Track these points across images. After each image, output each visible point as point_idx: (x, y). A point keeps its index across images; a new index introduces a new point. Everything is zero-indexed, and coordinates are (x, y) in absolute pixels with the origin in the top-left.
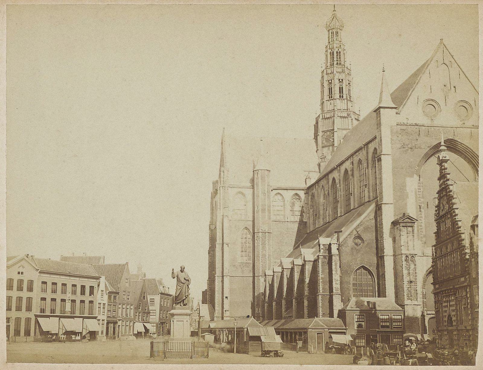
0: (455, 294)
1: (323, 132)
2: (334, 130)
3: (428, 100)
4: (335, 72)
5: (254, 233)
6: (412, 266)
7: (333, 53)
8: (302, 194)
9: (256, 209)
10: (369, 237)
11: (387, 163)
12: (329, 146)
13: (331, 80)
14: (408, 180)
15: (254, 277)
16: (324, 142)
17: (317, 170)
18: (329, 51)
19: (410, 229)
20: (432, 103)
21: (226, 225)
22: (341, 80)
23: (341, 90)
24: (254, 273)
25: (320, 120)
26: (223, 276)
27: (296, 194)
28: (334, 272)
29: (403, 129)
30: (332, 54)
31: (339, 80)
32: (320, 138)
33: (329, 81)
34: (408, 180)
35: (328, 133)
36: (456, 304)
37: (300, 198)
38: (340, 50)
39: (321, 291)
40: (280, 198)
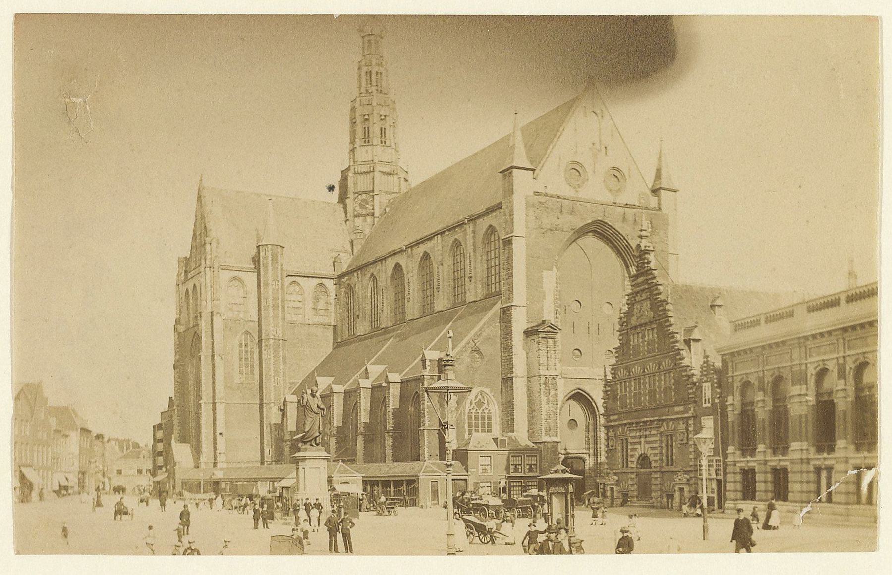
1: (355, 193)
2: (373, 191)
3: (614, 168)
4: (374, 104)
5: (260, 341)
6: (552, 392)
8: (329, 284)
9: (263, 303)
10: (493, 350)
11: (519, 249)
12: (365, 216)
15: (261, 405)
16: (357, 208)
17: (349, 247)
18: (365, 69)
20: (576, 169)
23: (383, 131)
24: (261, 400)
25: (350, 174)
26: (214, 404)
27: (321, 285)
29: (542, 201)
34: (545, 273)
35: (364, 196)
36: (661, 441)
37: (326, 292)
38: (382, 70)
39: (427, 425)
40: (297, 288)
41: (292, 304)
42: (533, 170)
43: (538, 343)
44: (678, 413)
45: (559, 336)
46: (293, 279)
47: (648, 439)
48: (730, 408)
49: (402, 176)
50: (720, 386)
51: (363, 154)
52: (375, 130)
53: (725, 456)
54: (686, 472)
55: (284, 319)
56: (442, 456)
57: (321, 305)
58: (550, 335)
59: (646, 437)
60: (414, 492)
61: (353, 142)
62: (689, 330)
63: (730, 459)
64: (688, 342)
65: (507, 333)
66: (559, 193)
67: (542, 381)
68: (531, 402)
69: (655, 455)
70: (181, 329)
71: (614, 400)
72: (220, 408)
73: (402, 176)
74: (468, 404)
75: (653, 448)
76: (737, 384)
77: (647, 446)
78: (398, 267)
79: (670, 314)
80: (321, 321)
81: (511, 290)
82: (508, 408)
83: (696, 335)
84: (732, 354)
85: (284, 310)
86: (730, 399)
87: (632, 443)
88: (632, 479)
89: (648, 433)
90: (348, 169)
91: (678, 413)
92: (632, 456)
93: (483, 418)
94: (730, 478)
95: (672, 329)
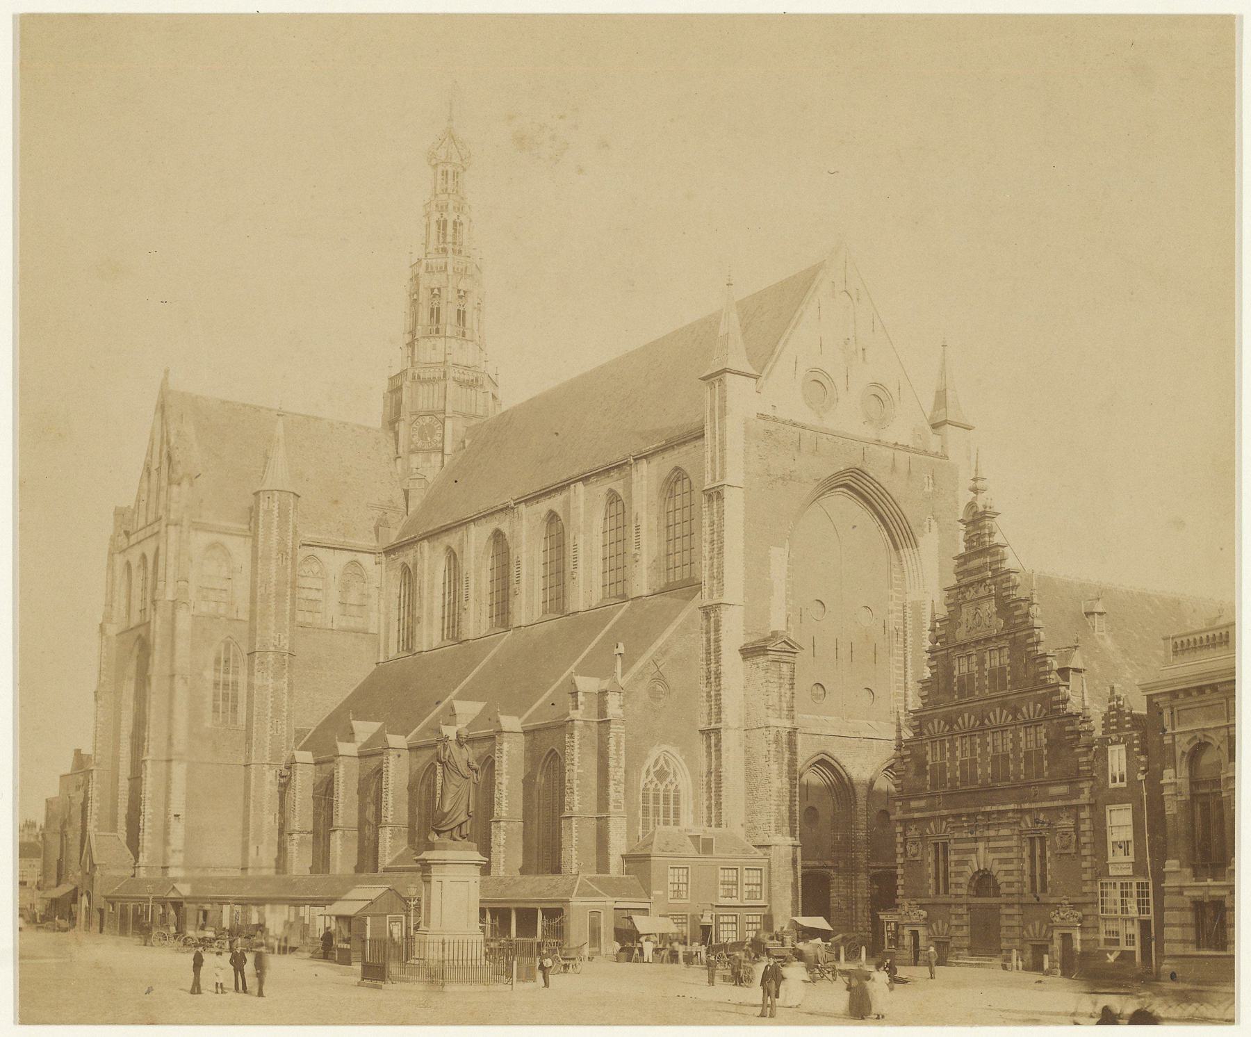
0: (1018, 823)
7: (445, 221)
9: (260, 591)
12: (429, 451)
13: (439, 290)
14: (774, 551)
16: (415, 439)
19: (785, 668)
21: (184, 622)
22: (436, 291)
27: (355, 563)
28: (612, 763)
30: (442, 225)
31: (459, 291)
32: (402, 427)
33: (432, 290)
34: (774, 551)
38: (462, 218)
40: (316, 568)
41: (305, 594)
42: (757, 378)
43: (767, 670)
44: (1053, 798)
45: (798, 659)
46: (309, 551)
47: (992, 844)
48: (1167, 792)
49: (490, 388)
50: (1144, 751)
51: (430, 351)
52: (449, 315)
53: (1159, 876)
54: (1076, 906)
55: (293, 619)
56: (603, 866)
57: (353, 598)
58: (785, 656)
59: (988, 839)
60: (558, 931)
61: (412, 333)
62: (1067, 656)
63: (1169, 883)
64: (1063, 672)
65: (713, 652)
66: (796, 419)
67: (771, 737)
68: (750, 773)
69: (1008, 873)
70: (112, 630)
71: (917, 774)
72: (179, 770)
73: (490, 388)
74: (644, 775)
75: (1002, 861)
76: (1183, 745)
77: (991, 856)
78: (498, 535)
79: (1037, 622)
80: (352, 624)
81: (718, 577)
82: (714, 782)
83: (1076, 661)
84: (1174, 694)
85: (293, 603)
86: (1168, 776)
87: (957, 852)
88: (960, 916)
89: (992, 833)
90: (403, 373)
91: (1053, 798)
92: (959, 874)
93: (666, 798)
94: (1169, 916)
95: (1041, 649)
